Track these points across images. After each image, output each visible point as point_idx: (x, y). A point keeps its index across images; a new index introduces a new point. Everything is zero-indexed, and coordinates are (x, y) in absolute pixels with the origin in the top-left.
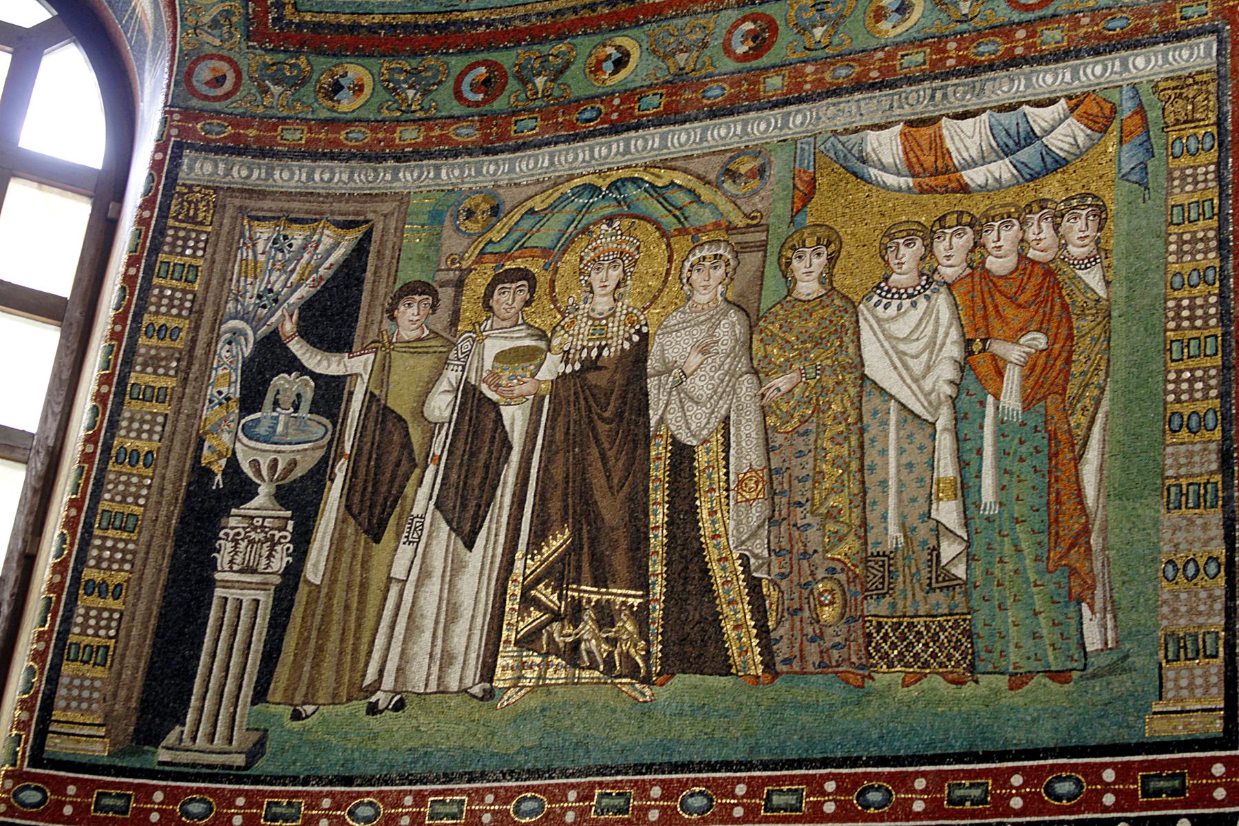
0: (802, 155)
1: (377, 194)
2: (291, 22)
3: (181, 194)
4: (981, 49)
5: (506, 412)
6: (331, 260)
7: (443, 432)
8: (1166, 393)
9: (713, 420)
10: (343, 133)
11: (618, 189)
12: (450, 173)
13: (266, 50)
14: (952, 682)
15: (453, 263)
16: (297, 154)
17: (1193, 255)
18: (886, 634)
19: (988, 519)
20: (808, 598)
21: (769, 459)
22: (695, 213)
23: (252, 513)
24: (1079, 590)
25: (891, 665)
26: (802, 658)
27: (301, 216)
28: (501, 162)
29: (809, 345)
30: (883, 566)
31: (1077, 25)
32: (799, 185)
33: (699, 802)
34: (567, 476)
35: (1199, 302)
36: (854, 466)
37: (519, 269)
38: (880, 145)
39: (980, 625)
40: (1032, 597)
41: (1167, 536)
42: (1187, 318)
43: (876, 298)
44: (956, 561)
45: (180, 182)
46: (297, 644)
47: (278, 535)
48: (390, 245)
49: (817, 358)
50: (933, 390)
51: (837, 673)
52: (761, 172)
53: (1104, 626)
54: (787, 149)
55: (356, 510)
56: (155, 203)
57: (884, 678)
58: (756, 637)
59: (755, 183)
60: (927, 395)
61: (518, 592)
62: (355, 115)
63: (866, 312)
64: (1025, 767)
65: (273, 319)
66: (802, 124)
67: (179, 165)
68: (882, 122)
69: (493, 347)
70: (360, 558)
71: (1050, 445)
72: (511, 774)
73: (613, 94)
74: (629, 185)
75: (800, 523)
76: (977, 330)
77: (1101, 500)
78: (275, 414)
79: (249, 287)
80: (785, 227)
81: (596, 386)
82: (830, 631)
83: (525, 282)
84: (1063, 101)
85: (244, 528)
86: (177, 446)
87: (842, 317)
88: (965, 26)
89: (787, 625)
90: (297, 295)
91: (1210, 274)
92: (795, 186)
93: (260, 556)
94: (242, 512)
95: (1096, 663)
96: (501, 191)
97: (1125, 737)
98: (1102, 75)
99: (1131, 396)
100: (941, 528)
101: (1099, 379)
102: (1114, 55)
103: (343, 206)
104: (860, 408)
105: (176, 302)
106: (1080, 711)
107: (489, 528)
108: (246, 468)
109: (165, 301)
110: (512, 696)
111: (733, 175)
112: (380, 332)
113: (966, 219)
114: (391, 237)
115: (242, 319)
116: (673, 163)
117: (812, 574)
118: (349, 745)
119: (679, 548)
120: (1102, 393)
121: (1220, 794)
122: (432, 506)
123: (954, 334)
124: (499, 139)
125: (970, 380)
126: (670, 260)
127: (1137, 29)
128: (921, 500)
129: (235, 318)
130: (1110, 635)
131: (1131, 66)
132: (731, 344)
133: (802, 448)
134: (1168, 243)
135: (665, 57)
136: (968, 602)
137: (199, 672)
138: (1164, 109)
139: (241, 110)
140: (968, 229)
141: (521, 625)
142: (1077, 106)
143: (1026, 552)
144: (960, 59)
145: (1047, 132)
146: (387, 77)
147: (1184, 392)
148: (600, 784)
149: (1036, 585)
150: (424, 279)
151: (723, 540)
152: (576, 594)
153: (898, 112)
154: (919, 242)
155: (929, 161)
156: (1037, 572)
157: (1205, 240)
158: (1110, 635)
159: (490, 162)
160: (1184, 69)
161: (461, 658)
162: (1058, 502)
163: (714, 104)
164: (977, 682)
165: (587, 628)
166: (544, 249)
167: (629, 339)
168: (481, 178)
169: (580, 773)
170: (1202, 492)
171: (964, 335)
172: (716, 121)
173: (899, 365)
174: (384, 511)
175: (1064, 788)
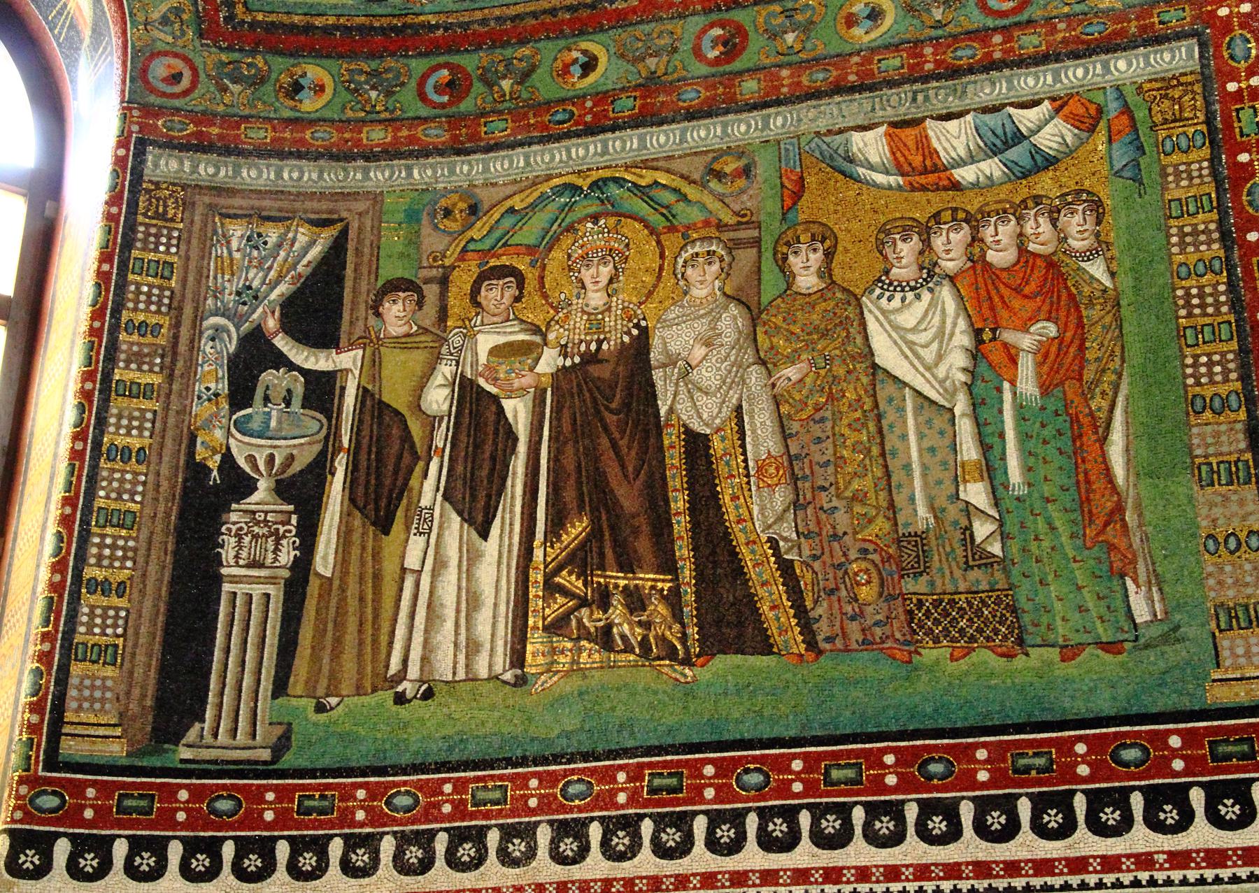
1: (349, 194)
2: (243, 21)
3: (148, 191)
4: (959, 53)
5: (508, 405)
6: (309, 257)
7: (444, 425)
8: (1185, 376)
9: (725, 409)
11: (599, 188)
12: (422, 173)
13: (220, 48)
14: (1002, 655)
15: (435, 260)
16: (262, 152)
18: (928, 610)
19: (1018, 499)
21: (787, 446)
22: (683, 211)
23: (253, 507)
26: (844, 633)
27: (273, 214)
28: (474, 163)
29: (815, 337)
30: (916, 546)
31: (1054, 30)
32: (787, 184)
33: (755, 779)
34: (580, 465)
36: (875, 451)
38: (866, 145)
40: (1072, 572)
41: (1204, 511)
43: (878, 291)
44: (990, 539)
45: (146, 178)
46: (314, 637)
48: (367, 242)
49: (825, 349)
50: (947, 378)
51: (882, 649)
52: (746, 172)
54: (770, 150)
56: (122, 198)
57: (930, 654)
58: (794, 616)
59: (741, 183)
60: (941, 382)
61: (540, 578)
62: (318, 114)
63: (869, 304)
65: (255, 316)
66: (783, 126)
67: (143, 162)
68: (866, 123)
69: (486, 343)
70: (370, 550)
72: (556, 759)
77: (1131, 479)
78: (267, 409)
79: (227, 284)
82: (869, 610)
84: (1046, 103)
86: (169, 442)
88: (940, 32)
89: (825, 604)
91: (1217, 264)
92: (783, 186)
94: (243, 507)
95: (1147, 634)
97: (1186, 704)
98: (1085, 77)
99: (1151, 380)
100: (971, 508)
103: (315, 205)
104: (874, 395)
105: (154, 299)
106: (1138, 680)
107: (503, 518)
108: (241, 462)
109: (143, 298)
111: (719, 176)
113: (961, 215)
114: (368, 235)
115: (223, 315)
116: (655, 164)
117: (845, 555)
118: (379, 736)
122: (439, 498)
123: (962, 324)
124: (469, 141)
125: (983, 368)
126: (662, 256)
127: (1116, 33)
130: (1158, 606)
132: (734, 336)
133: (820, 434)
134: (1169, 236)
136: (1008, 577)
138: (1150, 110)
139: (201, 108)
140: (964, 225)
141: (547, 611)
142: (1062, 107)
143: (1060, 530)
147: (1203, 375)
148: (650, 765)
149: (1075, 561)
150: (407, 276)
151: (749, 524)
152: (602, 580)
153: (881, 113)
154: (916, 238)
155: (917, 160)
156: (1076, 548)
158: (1158, 606)
159: (463, 163)
160: (1167, 71)
161: (488, 646)
162: (1088, 481)
163: (690, 106)
164: (1027, 655)
166: (528, 247)
167: (629, 333)
168: (454, 178)
169: (627, 752)
170: (1234, 469)
171: (972, 325)
172: (695, 123)
175: (1131, 754)
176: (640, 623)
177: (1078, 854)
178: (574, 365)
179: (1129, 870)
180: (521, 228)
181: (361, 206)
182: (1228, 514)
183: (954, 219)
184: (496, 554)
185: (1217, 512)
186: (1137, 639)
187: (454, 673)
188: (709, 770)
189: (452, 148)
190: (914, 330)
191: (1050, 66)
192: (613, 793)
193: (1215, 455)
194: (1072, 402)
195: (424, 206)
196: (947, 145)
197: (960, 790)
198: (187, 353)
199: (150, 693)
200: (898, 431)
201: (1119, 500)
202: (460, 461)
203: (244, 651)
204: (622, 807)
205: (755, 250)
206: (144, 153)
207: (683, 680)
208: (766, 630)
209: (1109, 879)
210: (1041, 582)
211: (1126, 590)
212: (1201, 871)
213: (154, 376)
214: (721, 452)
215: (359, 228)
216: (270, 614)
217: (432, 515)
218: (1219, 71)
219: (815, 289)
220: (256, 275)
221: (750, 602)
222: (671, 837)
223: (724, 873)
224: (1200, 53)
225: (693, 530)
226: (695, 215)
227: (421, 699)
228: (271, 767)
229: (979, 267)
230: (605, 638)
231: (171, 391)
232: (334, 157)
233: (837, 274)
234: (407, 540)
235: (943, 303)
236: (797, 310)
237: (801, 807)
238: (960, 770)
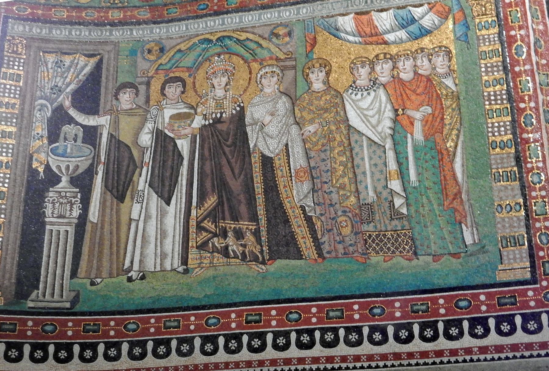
1: (103, 42)
3: (9, 40)
5: (179, 142)
7: (149, 152)
8: (488, 132)
11: (221, 41)
12: (137, 32)
14: (407, 259)
16: (61, 22)
18: (374, 239)
19: (414, 188)
21: (309, 163)
22: (260, 52)
23: (59, 190)
24: (460, 218)
26: (336, 250)
28: (162, 28)
30: (368, 209)
33: (294, 316)
34: (212, 171)
36: (350, 165)
37: (177, 77)
38: (344, 23)
39: (416, 234)
40: (438, 222)
41: (496, 194)
43: (350, 91)
44: (402, 207)
45: (8, 34)
47: (73, 200)
48: (112, 65)
50: (382, 132)
51: (352, 257)
52: (289, 34)
53: (473, 233)
57: (375, 259)
58: (312, 242)
59: (287, 39)
60: (380, 133)
61: (195, 224)
62: (88, 4)
63: (347, 97)
65: (60, 99)
66: (306, 13)
67: (7, 27)
69: (168, 113)
71: (438, 155)
72: (203, 307)
75: (327, 191)
78: (66, 144)
79: (46, 84)
80: (304, 59)
81: (221, 130)
82: (347, 238)
83: (180, 83)
84: (426, 5)
85: (56, 197)
86: (20, 159)
87: (336, 99)
89: (327, 236)
97: (488, 281)
100: (393, 192)
103: (88, 47)
104: (349, 139)
107: (177, 195)
111: (277, 36)
112: (112, 105)
113: (388, 56)
114: (112, 61)
115: (45, 99)
117: (336, 213)
118: (120, 296)
120: (460, 132)
123: (389, 107)
124: (159, 18)
126: (250, 73)
130: (476, 237)
132: (284, 111)
134: (481, 68)
138: (472, 10)
140: (389, 61)
142: (433, 7)
145: (421, 18)
147: (495, 132)
149: (440, 216)
150: (130, 81)
154: (367, 66)
156: (440, 211)
158: (476, 237)
162: (445, 179)
163: (263, 3)
164: (418, 259)
166: (188, 68)
167: (235, 109)
168: (152, 35)
170: (509, 175)
171: (393, 107)
172: (265, 11)
173: (365, 120)
175: (463, 304)
176: (241, 245)
177: (439, 349)
178: (210, 124)
179: (462, 355)
181: (109, 48)
182: (506, 195)
183: (385, 58)
184: (174, 212)
185: (502, 194)
188: (274, 313)
189: (151, 21)
190: (367, 109)
192: (229, 324)
193: (501, 168)
194: (438, 143)
197: (388, 321)
198: (29, 117)
199: (14, 276)
200: (360, 156)
203: (57, 257)
204: (234, 329)
207: (261, 271)
209: (453, 359)
212: (493, 355)
213: (13, 128)
219: (322, 90)
220: (60, 80)
222: (256, 343)
223: (280, 359)
225: (266, 202)
226: (265, 54)
227: (139, 280)
228: (70, 311)
229: (396, 80)
230: (225, 252)
237: (315, 329)
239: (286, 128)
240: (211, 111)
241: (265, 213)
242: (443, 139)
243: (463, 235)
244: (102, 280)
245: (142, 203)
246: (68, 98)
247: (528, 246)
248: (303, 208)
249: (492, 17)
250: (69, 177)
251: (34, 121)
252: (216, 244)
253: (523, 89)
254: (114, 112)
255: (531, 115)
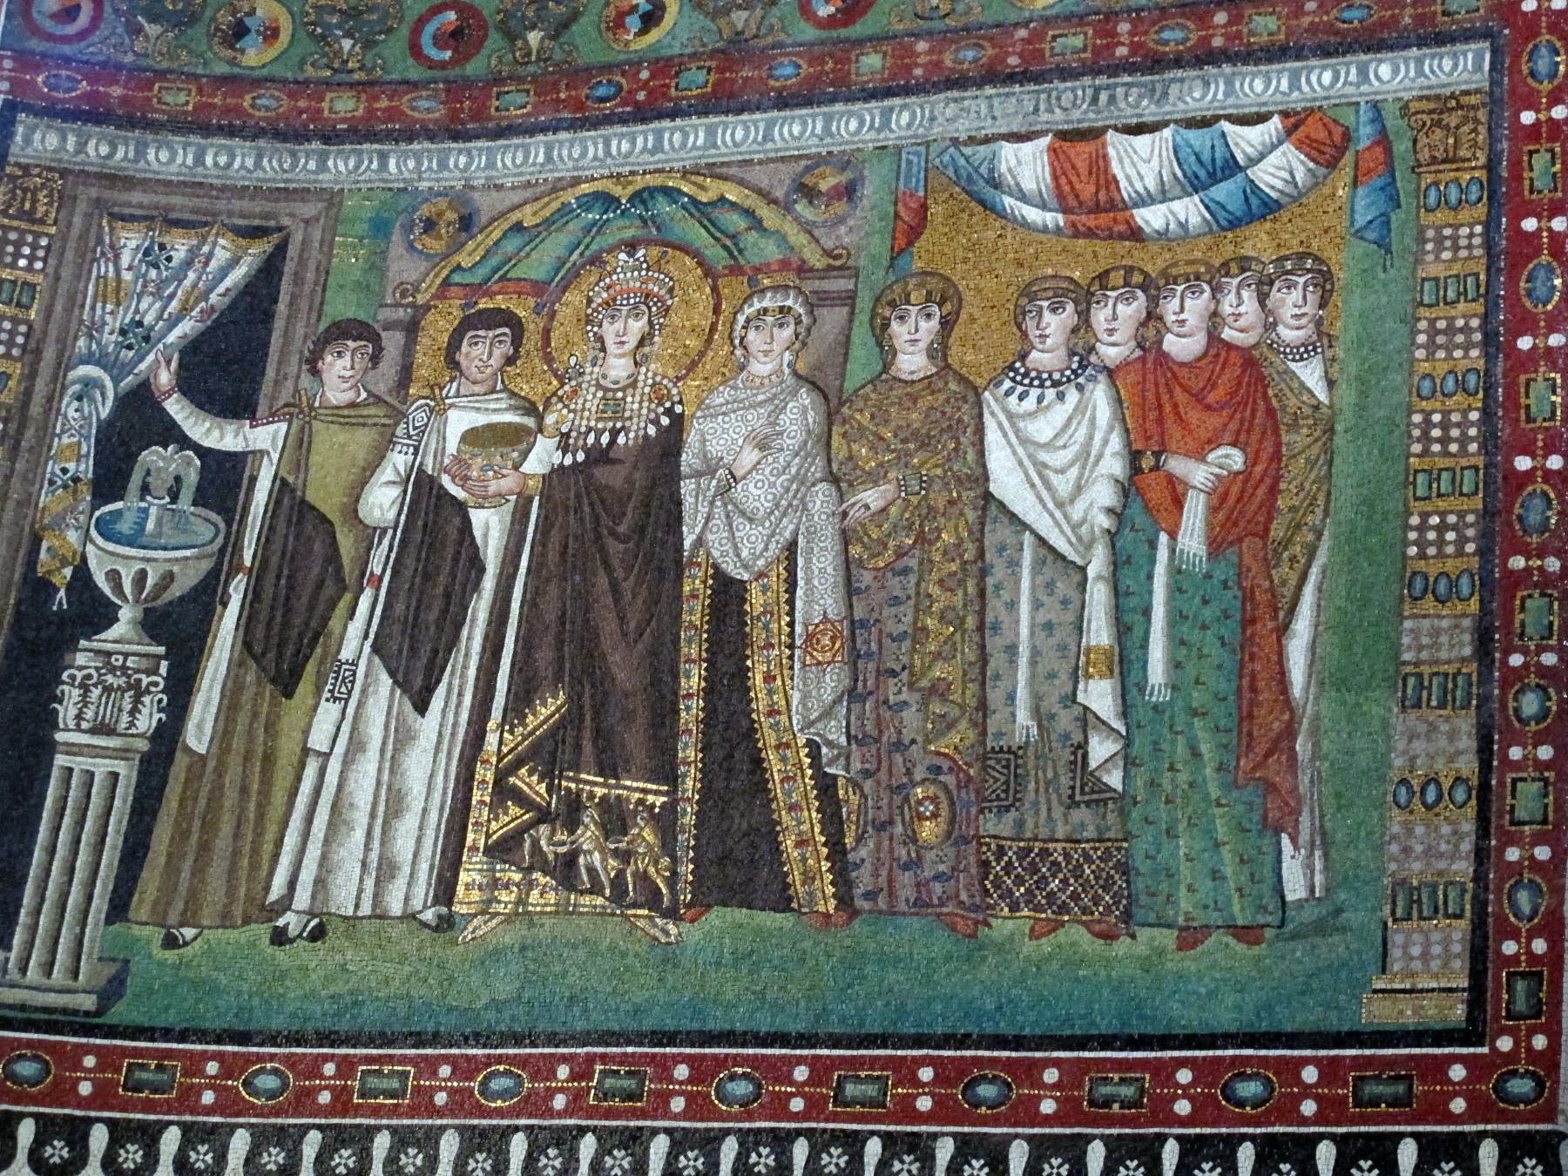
0: (909, 170)
1: (295, 190)
3: (13, 178)
4: (1166, 35)
5: (478, 517)
7: (386, 542)
9: (772, 546)
10: (248, 97)
11: (644, 202)
14: (1099, 935)
15: (403, 295)
17: (1449, 352)
18: (1010, 863)
19: (1155, 707)
20: (901, 808)
21: (851, 606)
22: (755, 244)
23: (109, 646)
24: (1278, 815)
25: (1014, 908)
27: (186, 216)
28: (475, 153)
30: (1007, 767)
33: (742, 1088)
34: (564, 614)
35: (1455, 417)
36: (971, 622)
38: (1019, 163)
41: (1401, 745)
42: (1438, 440)
43: (1007, 384)
44: (1110, 764)
45: (12, 159)
46: (172, 839)
47: (145, 680)
48: (312, 265)
50: (1084, 521)
51: (939, 915)
52: (849, 192)
53: (1309, 867)
55: (258, 649)
57: (1004, 926)
59: (840, 207)
60: (1075, 527)
61: (490, 777)
62: (265, 72)
63: (992, 403)
64: (1195, 1059)
65: (142, 366)
66: (909, 125)
68: (1023, 130)
69: (459, 422)
70: (263, 717)
71: (1244, 609)
72: (478, 1038)
73: (639, 63)
74: (661, 200)
76: (1148, 438)
77: (1312, 689)
78: (143, 505)
81: (607, 487)
83: (507, 330)
84: (1276, 118)
85: (97, 669)
90: (178, 332)
91: (1472, 380)
92: (897, 216)
93: (120, 710)
95: (1296, 919)
96: (476, 195)
97: (1335, 1022)
98: (1333, 85)
100: (1090, 716)
101: (1314, 519)
102: (1349, 58)
103: (246, 205)
104: (981, 541)
106: (1274, 984)
107: (450, 684)
108: (100, 580)
110: (480, 927)
111: (809, 193)
112: (297, 391)
114: (315, 253)
115: (98, 363)
117: (909, 773)
118: (245, 987)
119: (720, 727)
121: (1458, 1105)
122: (367, 649)
123: (1116, 442)
124: (473, 119)
125: (1136, 507)
126: (717, 311)
127: (1383, 24)
128: (1064, 676)
129: (88, 363)
131: (1372, 76)
132: (800, 437)
134: (1414, 332)
135: (716, 14)
136: (1124, 824)
137: (32, 873)
138: (1415, 142)
139: (101, 58)
140: (1139, 293)
142: (1296, 126)
143: (1206, 757)
144: (1135, 48)
145: (1253, 162)
146: (313, 18)
147: (1431, 543)
148: (604, 1058)
149: (1219, 805)
150: (362, 316)
151: (784, 718)
152: (573, 786)
154: (1070, 307)
156: (1223, 786)
157: (1466, 330)
159: (460, 152)
160: (1444, 86)
161: (407, 870)
162: (1253, 689)
163: (784, 88)
164: (1133, 937)
165: (588, 835)
166: (535, 283)
167: (656, 422)
168: (446, 174)
170: (1450, 685)
171: (1129, 444)
172: (788, 113)
174: (298, 652)
180: (528, 255)
181: (309, 209)
182: (1431, 750)
184: (434, 737)
185: (1419, 746)
186: (1282, 925)
187: (357, 906)
188: (682, 1071)
189: (448, 130)
190: (1047, 446)
191: (1289, 65)
194: (1249, 570)
195: (399, 214)
196: (1132, 172)
200: (1006, 596)
201: (1292, 718)
202: (402, 594)
204: (560, 1115)
205: (845, 310)
206: (13, 122)
208: (786, 874)
210: (1168, 832)
211: (1280, 852)
214: (759, 609)
215: (304, 242)
216: (116, 803)
217: (354, 675)
218: (1513, 91)
219: (922, 375)
220: (151, 306)
221: (770, 833)
224: (1492, 63)
226: (770, 251)
229: (1150, 358)
231: (12, 470)
232: (280, 136)
233: (955, 351)
234: (315, 708)
235: (1094, 408)
236: (893, 404)
237: (799, 1133)
238: (1019, 1096)
239: (798, 491)
240: (584, 422)
241: (700, 755)
242: (1265, 559)
243: (1280, 868)
244: (200, 934)
245: (347, 701)
246: (168, 363)
247: (1472, 921)
248: (813, 748)
249: (1473, 168)
250: (141, 608)
251: (58, 431)
252: (543, 843)
253: (1533, 409)
254: (301, 412)
255: (1545, 494)
